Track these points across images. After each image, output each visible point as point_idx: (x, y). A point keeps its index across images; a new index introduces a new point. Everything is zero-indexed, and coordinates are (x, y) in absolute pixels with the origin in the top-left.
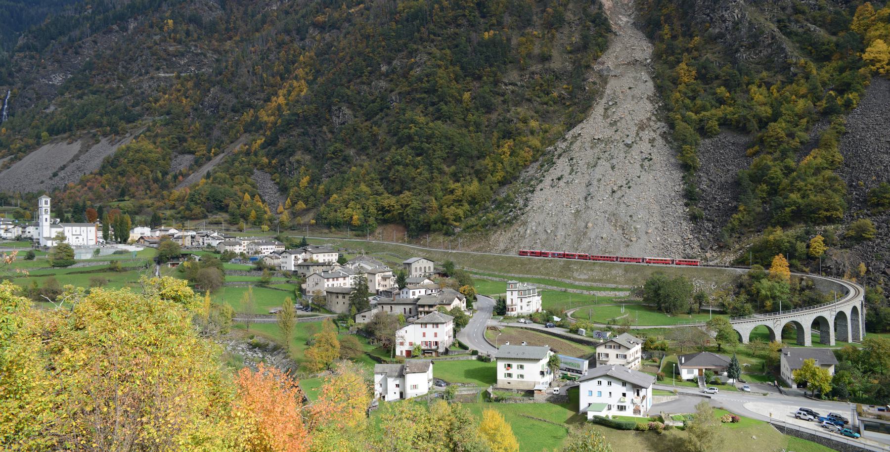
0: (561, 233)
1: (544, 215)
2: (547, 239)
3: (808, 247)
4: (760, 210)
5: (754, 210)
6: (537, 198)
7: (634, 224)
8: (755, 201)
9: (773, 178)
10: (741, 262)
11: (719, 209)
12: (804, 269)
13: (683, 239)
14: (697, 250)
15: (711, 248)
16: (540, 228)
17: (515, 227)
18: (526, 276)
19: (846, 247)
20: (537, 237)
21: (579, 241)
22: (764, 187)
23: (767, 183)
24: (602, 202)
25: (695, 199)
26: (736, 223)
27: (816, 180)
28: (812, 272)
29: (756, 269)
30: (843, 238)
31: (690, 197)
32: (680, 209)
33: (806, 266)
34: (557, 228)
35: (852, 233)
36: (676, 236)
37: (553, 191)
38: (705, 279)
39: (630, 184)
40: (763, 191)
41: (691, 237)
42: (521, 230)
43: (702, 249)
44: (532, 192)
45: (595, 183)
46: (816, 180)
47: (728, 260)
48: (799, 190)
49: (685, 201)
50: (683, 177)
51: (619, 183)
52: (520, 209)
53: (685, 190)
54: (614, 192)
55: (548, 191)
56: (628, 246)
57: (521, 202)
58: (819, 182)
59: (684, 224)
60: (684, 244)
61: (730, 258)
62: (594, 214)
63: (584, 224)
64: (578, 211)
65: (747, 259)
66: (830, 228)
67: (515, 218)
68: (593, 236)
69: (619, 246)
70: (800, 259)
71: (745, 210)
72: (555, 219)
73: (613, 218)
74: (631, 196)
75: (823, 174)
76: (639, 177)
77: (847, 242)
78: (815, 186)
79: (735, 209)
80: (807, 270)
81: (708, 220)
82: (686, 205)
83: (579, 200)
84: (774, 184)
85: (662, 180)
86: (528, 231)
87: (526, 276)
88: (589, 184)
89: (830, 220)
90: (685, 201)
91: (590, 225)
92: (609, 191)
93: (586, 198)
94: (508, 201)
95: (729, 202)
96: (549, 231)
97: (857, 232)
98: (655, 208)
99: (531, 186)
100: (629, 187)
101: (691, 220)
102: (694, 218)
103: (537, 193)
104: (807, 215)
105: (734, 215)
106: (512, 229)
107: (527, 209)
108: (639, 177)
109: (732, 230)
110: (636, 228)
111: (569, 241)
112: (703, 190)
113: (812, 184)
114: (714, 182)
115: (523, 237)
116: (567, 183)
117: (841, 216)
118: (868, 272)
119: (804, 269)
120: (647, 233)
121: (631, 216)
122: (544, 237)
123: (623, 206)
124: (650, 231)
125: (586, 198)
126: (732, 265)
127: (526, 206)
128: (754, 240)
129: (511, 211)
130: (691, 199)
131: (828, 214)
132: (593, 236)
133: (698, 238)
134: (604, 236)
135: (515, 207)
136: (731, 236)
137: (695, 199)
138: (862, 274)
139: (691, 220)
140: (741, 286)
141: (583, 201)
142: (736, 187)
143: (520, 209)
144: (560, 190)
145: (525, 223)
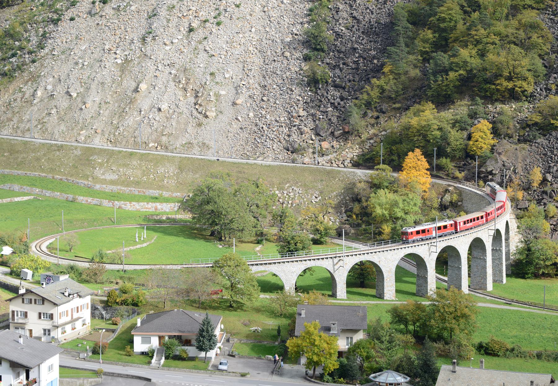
0: (94, 98)
1: (71, 63)
2: (70, 108)
3: (469, 138)
4: (415, 73)
5: (406, 73)
6: (63, 34)
7: (216, 89)
8: (411, 57)
9: (443, 20)
10: (366, 161)
11: (357, 69)
12: (457, 174)
13: (290, 117)
14: (308, 133)
15: (332, 133)
16: (59, 88)
17: (17, 83)
18: (15, 172)
19: (525, 141)
20: (53, 103)
21: (122, 114)
22: (429, 34)
23: (435, 28)
24: (170, 46)
25: (323, 50)
26: (375, 93)
27: (506, 26)
28: (467, 179)
29: (385, 172)
30: (525, 125)
31: (312, 45)
32: (295, 65)
33: (460, 169)
34: (88, 89)
35: (537, 118)
36: (281, 110)
37: (92, 22)
38: (305, 186)
39: (222, 18)
40: (425, 41)
41: (302, 113)
42: (28, 90)
43: (317, 134)
44: (56, 22)
45: (163, 13)
46: (506, 26)
47: (350, 155)
48: (478, 42)
49: (305, 51)
50: (311, 10)
51: (203, 14)
52: (30, 53)
53: (306, 33)
54: (191, 30)
55: (82, 23)
56: (200, 125)
57: (34, 40)
58: (510, 30)
59: (297, 90)
60: (291, 126)
61: (352, 151)
62: (153, 68)
63: (134, 85)
64: (127, 61)
65: (377, 155)
66: (508, 109)
67: (20, 68)
68: (145, 105)
69: (187, 124)
70: (453, 159)
71: (391, 72)
72: (87, 72)
73: (183, 77)
74: (219, 40)
75: (519, 16)
76: (238, 6)
77: (529, 131)
78: (503, 38)
79: (378, 71)
80: (461, 175)
81: (336, 86)
82: (306, 59)
83: (132, 41)
84: (444, 30)
85: (274, 14)
86: (39, 93)
87: (15, 172)
88: (153, 15)
89: (513, 96)
90: (305, 51)
91: (143, 87)
92: (184, 30)
93: (144, 39)
94: (12, 36)
95: (374, 58)
96: (74, 95)
97: (545, 118)
98: (258, 61)
99: (56, 12)
100: (218, 24)
101: (309, 84)
102: (313, 82)
103: (64, 25)
104: (480, 86)
105: (374, 81)
106: (12, 88)
107: (43, 52)
108: (238, 6)
109: (368, 105)
110: (218, 96)
111: (106, 113)
112: (338, 35)
113: (498, 34)
114: (358, 21)
115: (30, 103)
116: (118, 9)
117: (530, 89)
118: (545, 180)
119: (457, 174)
120: (234, 104)
121: (212, 74)
122: (64, 103)
123: (203, 56)
124: (239, 101)
125: (144, 39)
126: (356, 165)
127: (41, 46)
128: (393, 125)
129: (13, 55)
130: (316, 49)
131: (510, 85)
132: (145, 105)
133: (313, 115)
134: (164, 107)
135: (21, 48)
136: (365, 115)
137: (323, 50)
138: (535, 184)
139: (309, 84)
140: (357, 199)
141: (138, 44)
142: (385, 33)
143: (30, 53)
144: (104, 21)
145: (35, 78)
